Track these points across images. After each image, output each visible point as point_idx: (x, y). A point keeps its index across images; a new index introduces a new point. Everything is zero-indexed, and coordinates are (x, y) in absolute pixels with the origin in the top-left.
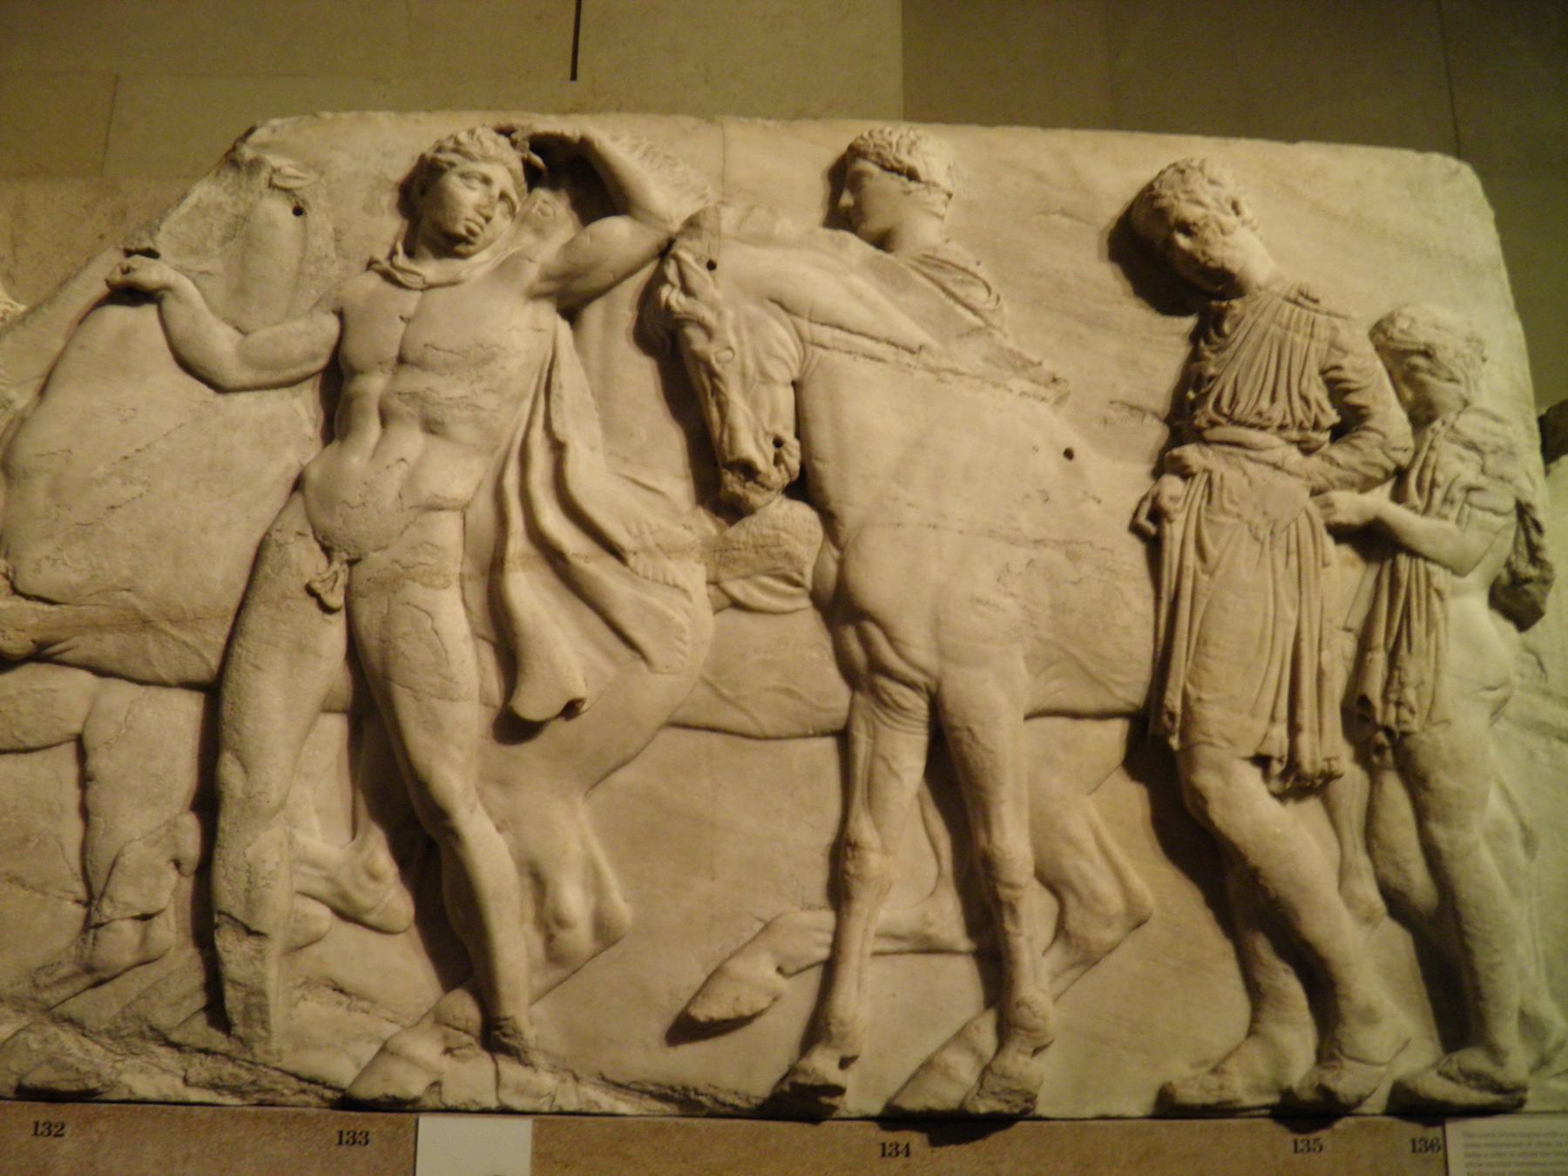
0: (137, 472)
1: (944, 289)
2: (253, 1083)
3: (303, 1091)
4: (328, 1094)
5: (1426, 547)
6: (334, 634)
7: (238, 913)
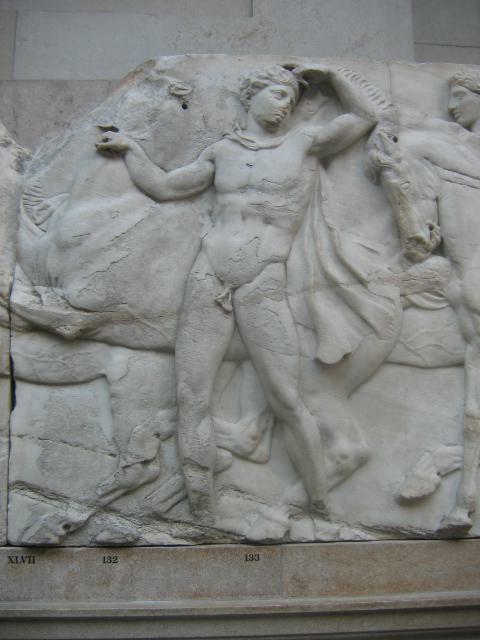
0: (123, 244)
2: (203, 535)
3: (225, 537)
4: (236, 538)
6: (228, 323)
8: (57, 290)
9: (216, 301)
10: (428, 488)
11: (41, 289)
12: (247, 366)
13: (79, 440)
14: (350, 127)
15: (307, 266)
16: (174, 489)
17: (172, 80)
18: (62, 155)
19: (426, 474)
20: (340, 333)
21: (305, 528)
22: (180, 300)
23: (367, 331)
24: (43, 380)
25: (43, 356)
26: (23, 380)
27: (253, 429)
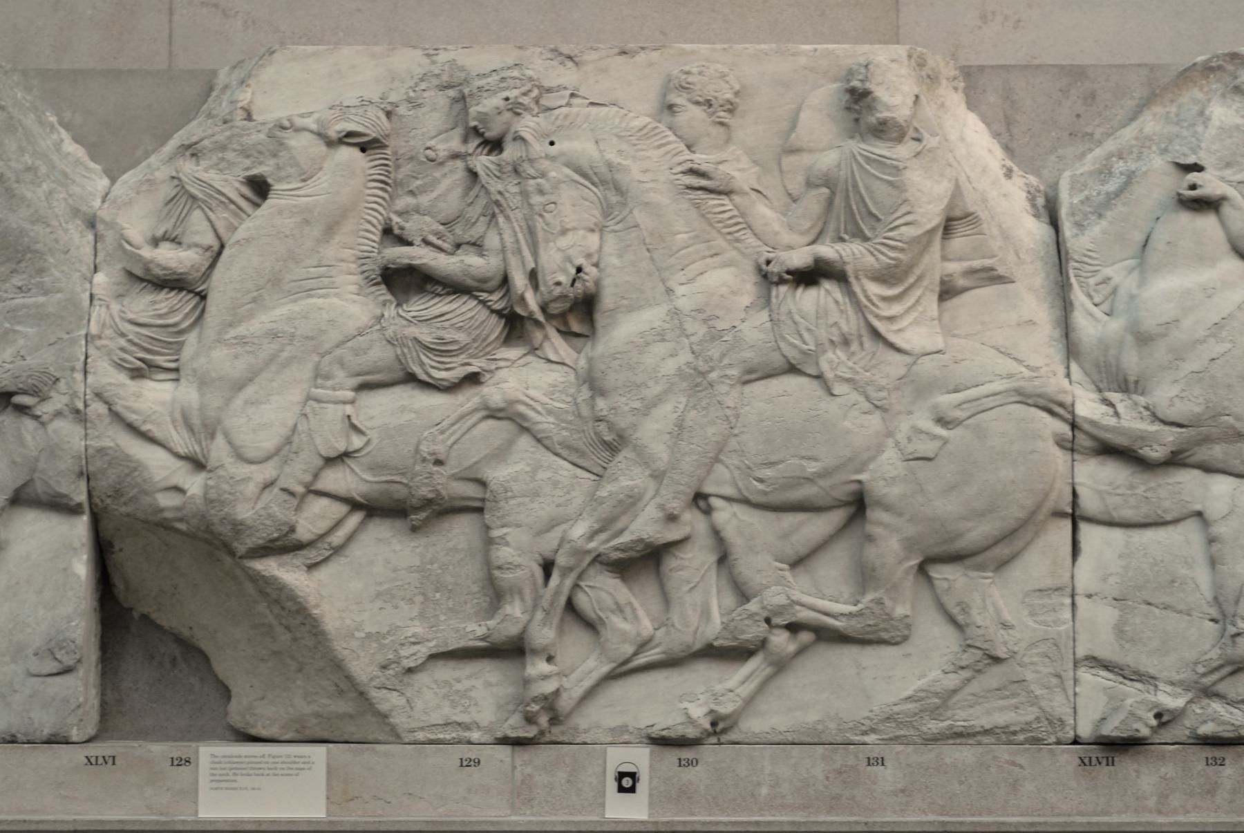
0: (1224, 334)
8: (1135, 397)
11: (1115, 397)
13: (1168, 600)
18: (1124, 204)
24: (1117, 520)
25: (1118, 487)
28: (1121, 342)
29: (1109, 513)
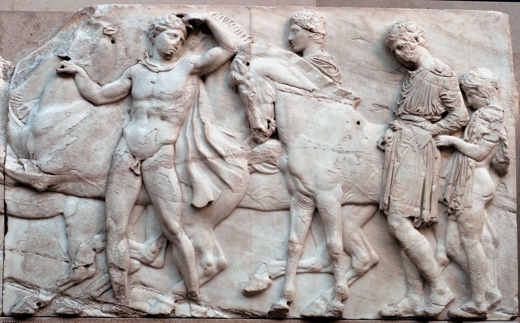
0: (74, 133)
1: (321, 70)
2: (121, 311)
3: (135, 313)
4: (142, 314)
5: (468, 153)
6: (138, 182)
7: (116, 263)
8: (33, 161)
9: (130, 168)
10: (262, 286)
11: (24, 161)
12: (150, 208)
13: (46, 252)
14: (217, 57)
15: (187, 147)
16: (104, 282)
17: (105, 24)
18: (35, 74)
19: (263, 278)
20: (207, 188)
21: (184, 309)
22: (109, 167)
23: (225, 187)
24: (24, 216)
25: (25, 201)
26: (12, 216)
27: (153, 247)
28: (27, 136)
29: (21, 213)
